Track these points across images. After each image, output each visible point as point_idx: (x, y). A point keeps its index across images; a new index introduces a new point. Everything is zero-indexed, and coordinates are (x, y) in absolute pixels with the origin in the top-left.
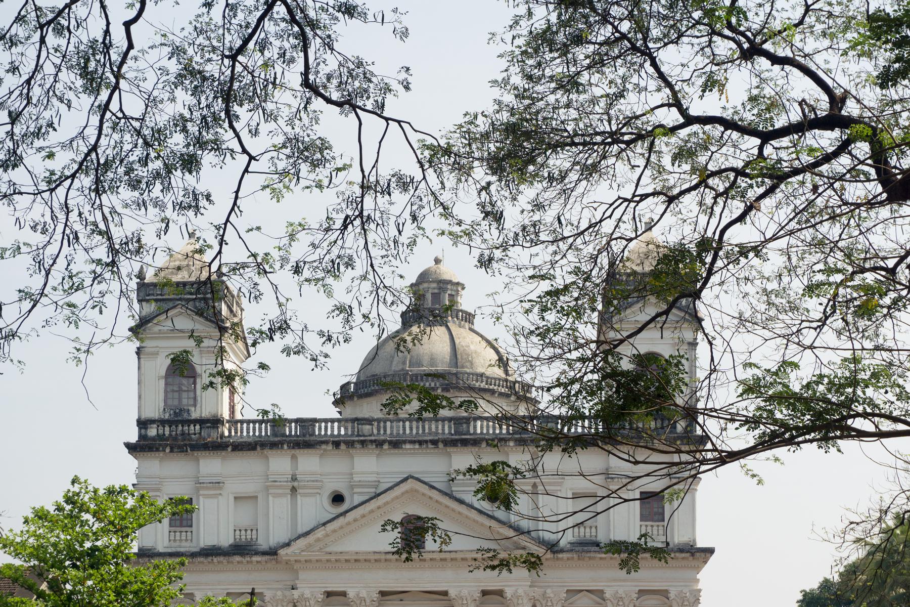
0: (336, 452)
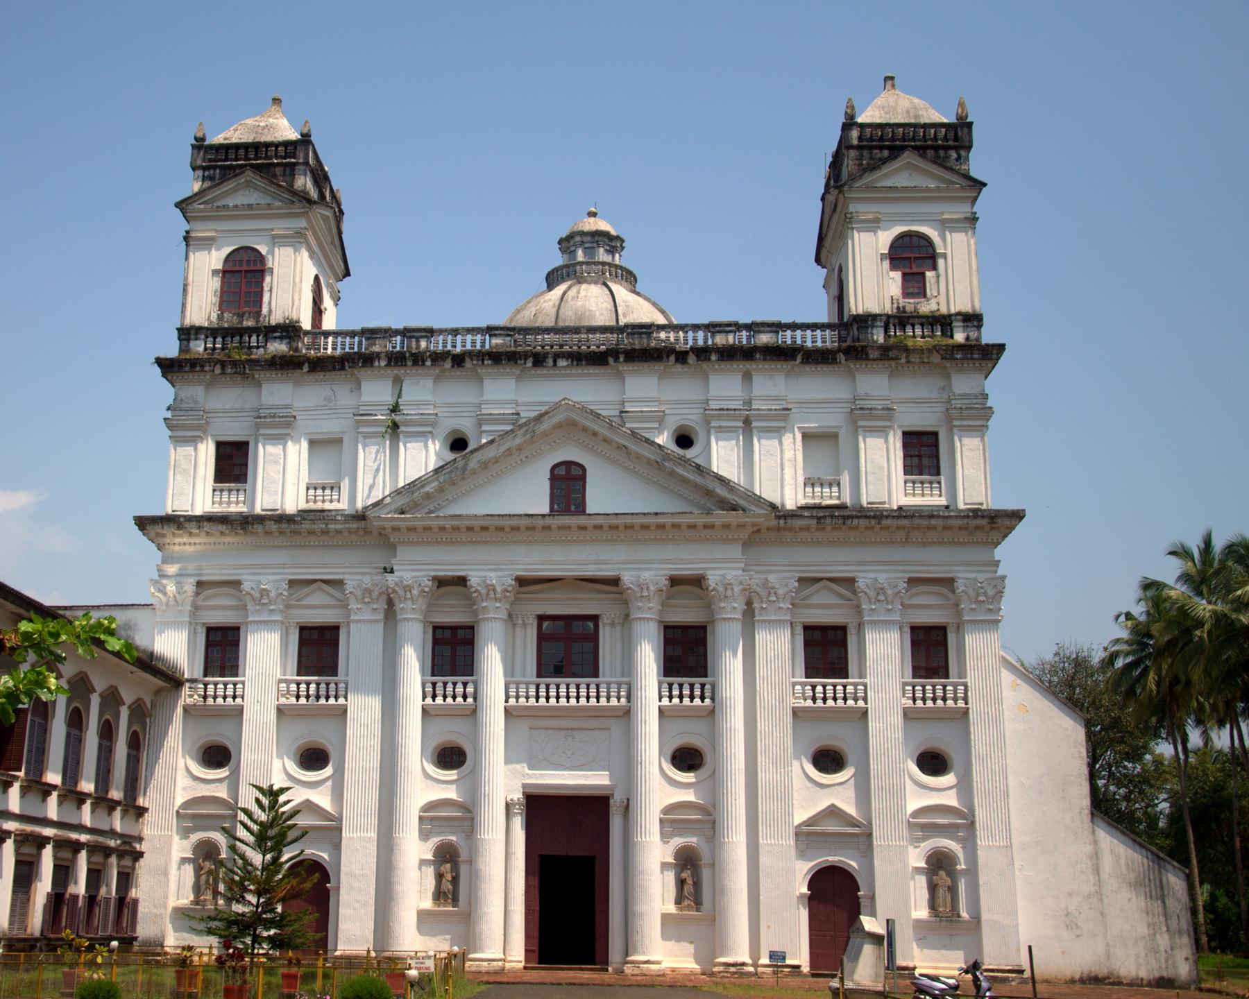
0: (458, 372)
